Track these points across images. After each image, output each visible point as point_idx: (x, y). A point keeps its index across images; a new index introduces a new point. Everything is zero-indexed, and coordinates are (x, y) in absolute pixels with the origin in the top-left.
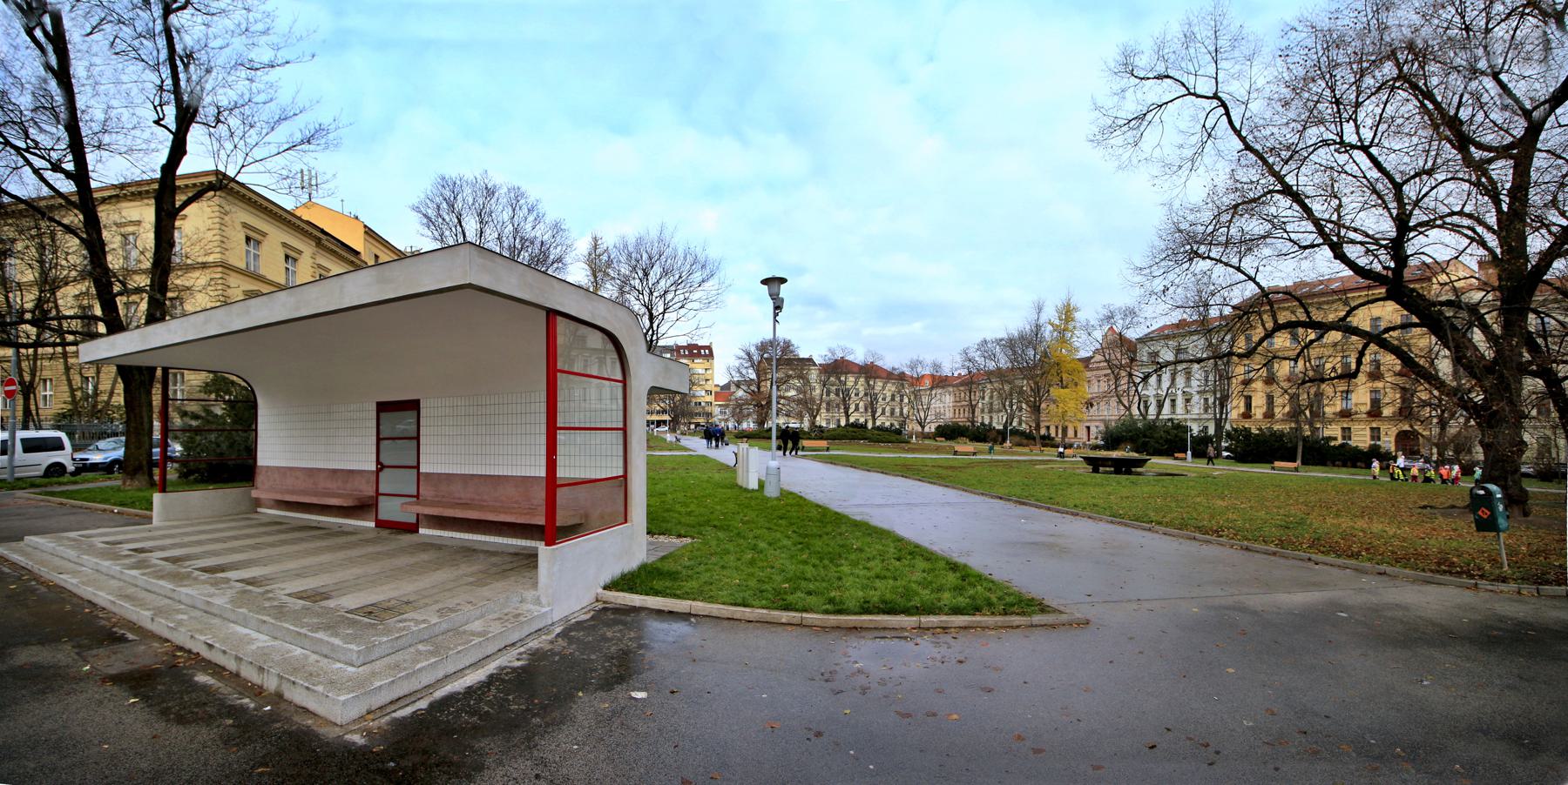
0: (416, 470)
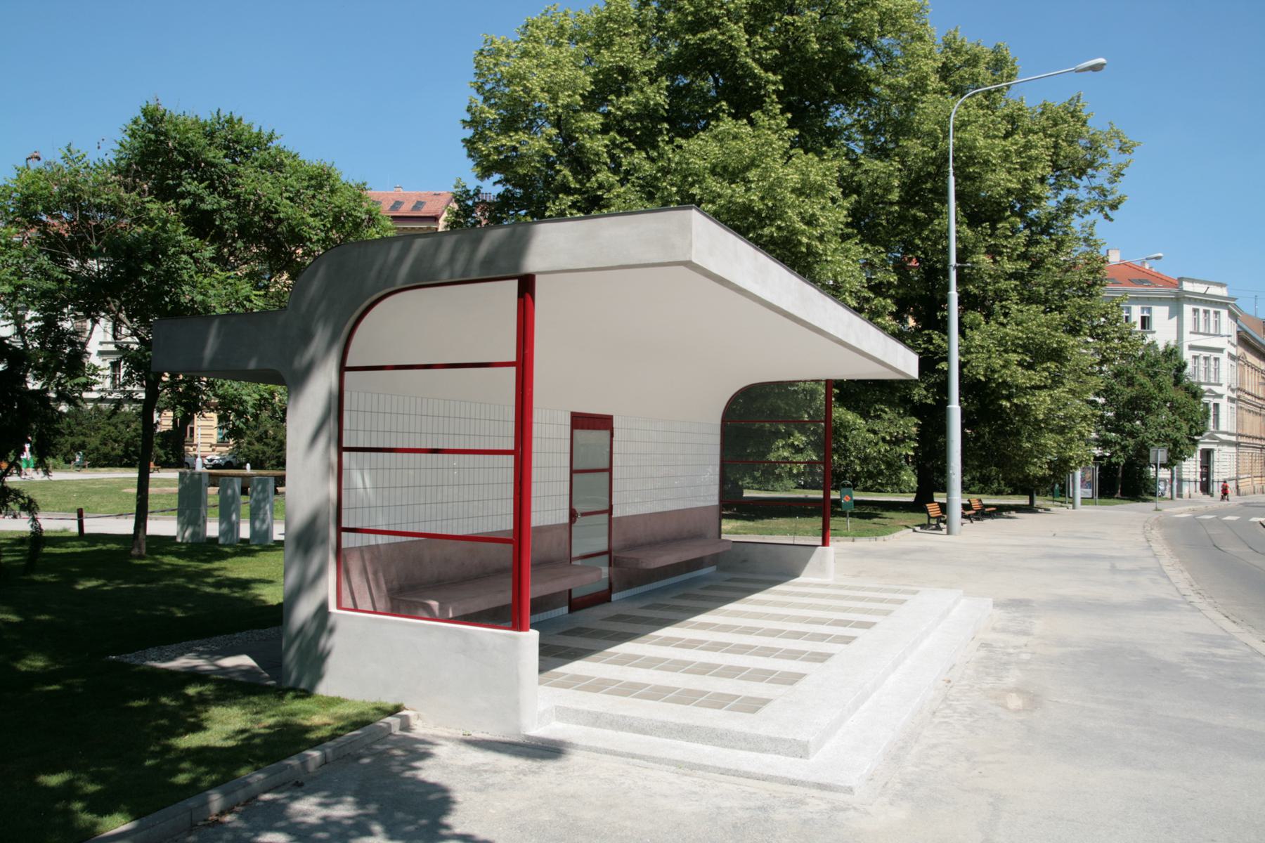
0: (606, 516)
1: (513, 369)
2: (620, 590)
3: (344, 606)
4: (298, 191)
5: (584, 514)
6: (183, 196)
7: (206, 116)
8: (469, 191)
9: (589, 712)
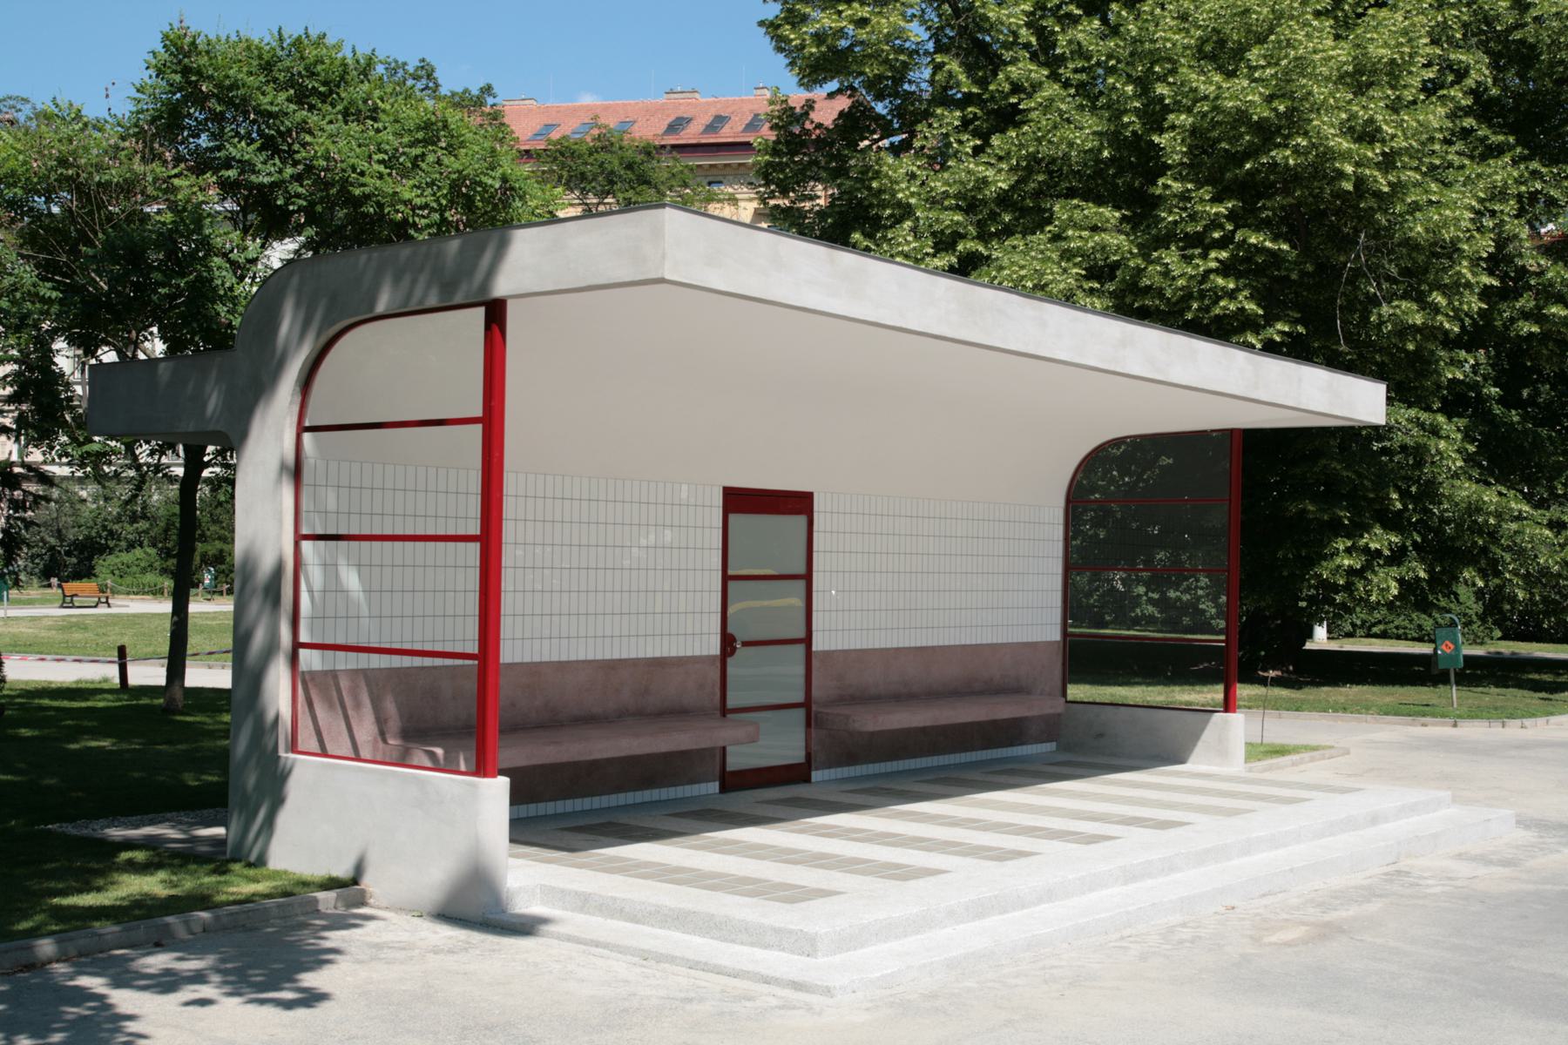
0: (800, 650)
1: (478, 428)
2: (829, 765)
3: (300, 749)
4: (397, 150)
5: (746, 644)
6: (228, 163)
7: (261, 33)
8: (793, 109)
9: (576, 893)
